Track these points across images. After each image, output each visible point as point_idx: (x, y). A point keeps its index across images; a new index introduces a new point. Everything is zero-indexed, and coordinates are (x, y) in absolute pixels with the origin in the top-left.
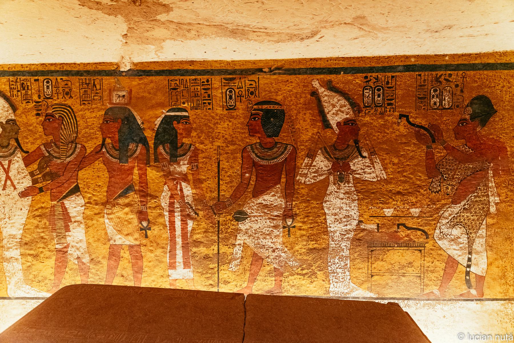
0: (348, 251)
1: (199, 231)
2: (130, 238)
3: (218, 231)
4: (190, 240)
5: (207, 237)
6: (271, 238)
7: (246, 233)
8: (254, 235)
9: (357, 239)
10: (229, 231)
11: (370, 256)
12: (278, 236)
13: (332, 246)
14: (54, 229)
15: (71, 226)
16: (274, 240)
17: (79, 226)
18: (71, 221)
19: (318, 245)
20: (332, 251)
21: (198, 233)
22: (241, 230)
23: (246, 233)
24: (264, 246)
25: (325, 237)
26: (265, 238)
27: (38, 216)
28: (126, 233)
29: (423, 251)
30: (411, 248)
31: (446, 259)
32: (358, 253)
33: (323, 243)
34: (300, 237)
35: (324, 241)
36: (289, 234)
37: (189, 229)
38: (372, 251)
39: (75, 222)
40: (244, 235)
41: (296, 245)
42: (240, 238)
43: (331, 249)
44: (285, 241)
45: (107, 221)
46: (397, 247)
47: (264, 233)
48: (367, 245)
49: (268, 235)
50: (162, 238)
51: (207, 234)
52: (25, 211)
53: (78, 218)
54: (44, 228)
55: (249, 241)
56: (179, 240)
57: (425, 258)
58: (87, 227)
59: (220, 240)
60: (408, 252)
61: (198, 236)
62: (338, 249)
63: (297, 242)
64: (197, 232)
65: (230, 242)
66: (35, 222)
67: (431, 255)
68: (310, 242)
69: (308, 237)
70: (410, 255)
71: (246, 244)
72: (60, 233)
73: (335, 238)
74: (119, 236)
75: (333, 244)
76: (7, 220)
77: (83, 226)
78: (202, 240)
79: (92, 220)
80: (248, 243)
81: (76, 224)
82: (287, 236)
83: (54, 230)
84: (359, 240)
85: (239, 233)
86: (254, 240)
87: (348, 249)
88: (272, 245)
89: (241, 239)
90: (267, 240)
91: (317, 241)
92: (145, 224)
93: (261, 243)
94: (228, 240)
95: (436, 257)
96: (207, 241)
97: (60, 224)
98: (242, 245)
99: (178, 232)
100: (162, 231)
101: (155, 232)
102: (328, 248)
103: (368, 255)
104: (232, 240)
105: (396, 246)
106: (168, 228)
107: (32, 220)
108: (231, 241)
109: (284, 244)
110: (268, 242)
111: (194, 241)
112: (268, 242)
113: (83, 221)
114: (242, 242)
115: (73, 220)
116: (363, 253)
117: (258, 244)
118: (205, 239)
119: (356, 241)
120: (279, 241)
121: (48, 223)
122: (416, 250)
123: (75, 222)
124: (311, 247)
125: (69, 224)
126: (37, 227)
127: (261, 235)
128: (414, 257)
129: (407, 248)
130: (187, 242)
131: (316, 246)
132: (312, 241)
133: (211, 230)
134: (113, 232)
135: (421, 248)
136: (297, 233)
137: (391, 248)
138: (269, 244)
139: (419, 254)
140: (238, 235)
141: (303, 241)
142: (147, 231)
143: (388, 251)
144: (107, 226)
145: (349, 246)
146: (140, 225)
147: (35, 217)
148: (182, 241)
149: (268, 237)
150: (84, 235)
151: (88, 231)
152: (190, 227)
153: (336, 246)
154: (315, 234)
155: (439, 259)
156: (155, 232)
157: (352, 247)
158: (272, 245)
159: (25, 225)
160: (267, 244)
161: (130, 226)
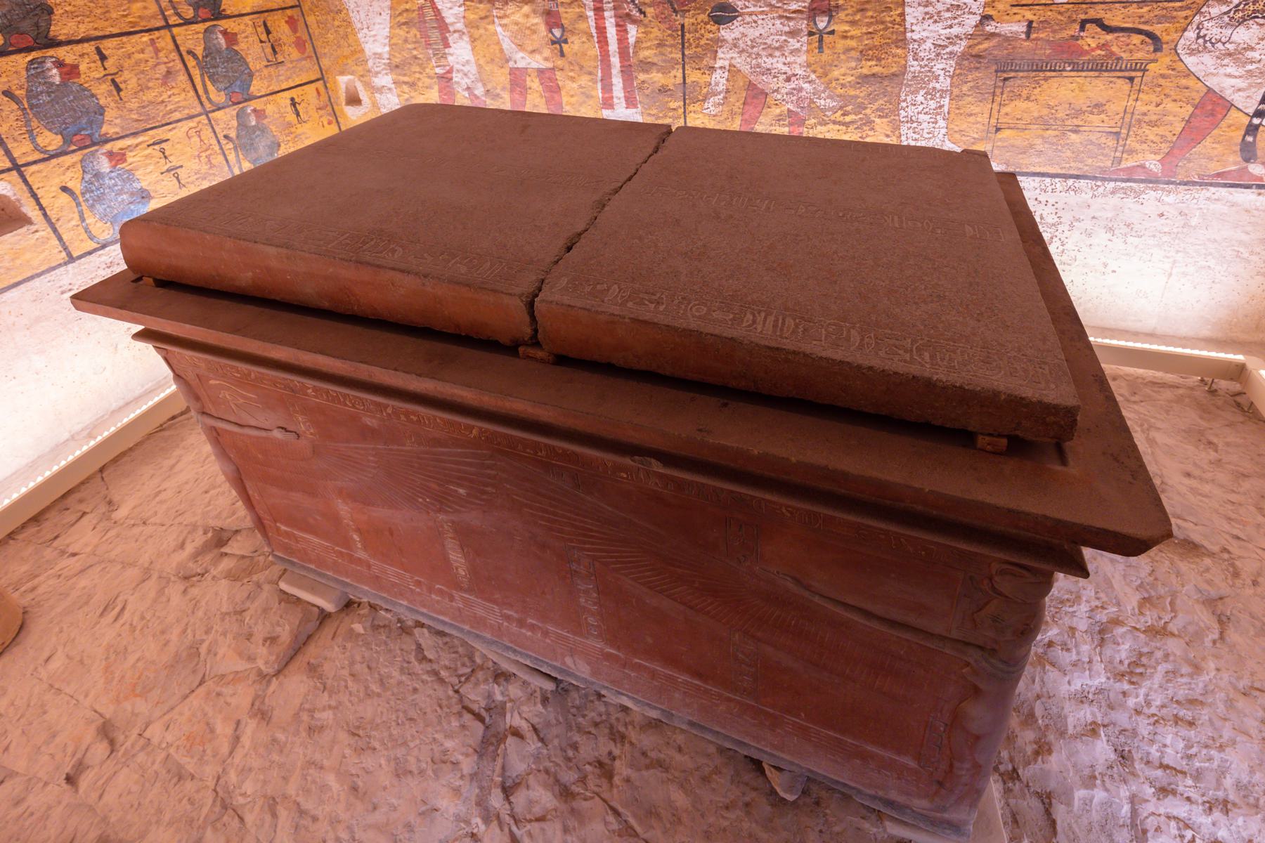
0: (949, 80)
1: (649, 44)
2: (538, 57)
3: (683, 44)
4: (633, 61)
5: (664, 55)
6: (783, 55)
7: (735, 46)
8: (750, 50)
9: (972, 56)
10: (703, 42)
11: (1000, 90)
12: (798, 50)
13: (912, 69)
14: (429, 44)
15: (450, 39)
16: (788, 59)
17: (461, 38)
18: (449, 32)
19: (881, 68)
20: (911, 81)
21: (648, 48)
22: (724, 40)
23: (735, 46)
24: (768, 69)
25: (899, 51)
26: (771, 55)
27: (404, 24)
28: (530, 48)
29: (1136, 81)
30: (1106, 74)
31: (1197, 98)
32: (972, 84)
33: (893, 65)
34: (844, 53)
35: (895, 59)
36: (820, 48)
37: (632, 40)
38: (1006, 79)
39: (455, 32)
40: (731, 49)
41: (834, 68)
42: (722, 56)
43: (909, 76)
44: (812, 60)
45: (499, 29)
46: (1071, 71)
47: (770, 47)
48: (994, 67)
49: (777, 49)
50: (587, 58)
51: (662, 50)
52: (386, 16)
53: (458, 25)
54: (415, 42)
55: (740, 62)
56: (615, 60)
57: (1141, 95)
58: (473, 40)
59: (687, 60)
60: (1098, 82)
61: (647, 53)
62: (926, 76)
63: (836, 63)
64: (644, 45)
65: (705, 62)
66: (402, 32)
67: (1159, 89)
68: (864, 62)
69: (861, 52)
70: (1103, 87)
71: (735, 67)
72: (438, 50)
73: (922, 54)
74: (521, 54)
75: (914, 66)
76: (365, 31)
77: (466, 38)
78: (655, 60)
79: (478, 27)
80: (738, 65)
81: (456, 35)
82: (817, 51)
83: (428, 45)
84: (978, 56)
85: (721, 47)
86: (749, 60)
87: (949, 76)
88: (785, 69)
89: (725, 57)
90: (775, 60)
91: (879, 59)
92: (557, 32)
93: (763, 65)
94: (701, 58)
95: (1172, 93)
96: (664, 61)
97: (435, 35)
98: (727, 68)
99: (613, 46)
100: (586, 46)
101: (576, 47)
102: (904, 74)
103: (995, 87)
104: (708, 59)
105: (1069, 69)
106: (596, 40)
107: (398, 31)
108: (707, 61)
109: (809, 65)
110: (777, 63)
111: (641, 61)
112: (777, 63)
113: (465, 31)
114: (726, 63)
115: (451, 29)
116: (984, 84)
117: (759, 66)
118: (660, 58)
119: (971, 59)
120: (799, 60)
121: (418, 36)
122: (1119, 77)
123: (455, 31)
124: (865, 71)
125: (447, 35)
126: (406, 41)
127: (763, 49)
128: (1110, 92)
129: (1096, 74)
130: (629, 63)
131: (876, 70)
132: (869, 60)
133: (670, 41)
134: (511, 48)
135: (1133, 74)
136: (837, 45)
137: (1053, 74)
138: (780, 66)
139: (1127, 87)
140: (720, 51)
141: (850, 60)
142: (563, 45)
143: (1046, 79)
144: (501, 37)
145: (952, 70)
146: (550, 35)
147: (400, 25)
148: (621, 62)
149: (777, 53)
150: (471, 53)
151: (475, 47)
152: (632, 37)
153: (922, 70)
154: (875, 46)
155: (1175, 98)
156: (576, 47)
157: (958, 72)
158: (785, 69)
159: (391, 38)
160: (775, 66)
161: (535, 37)
